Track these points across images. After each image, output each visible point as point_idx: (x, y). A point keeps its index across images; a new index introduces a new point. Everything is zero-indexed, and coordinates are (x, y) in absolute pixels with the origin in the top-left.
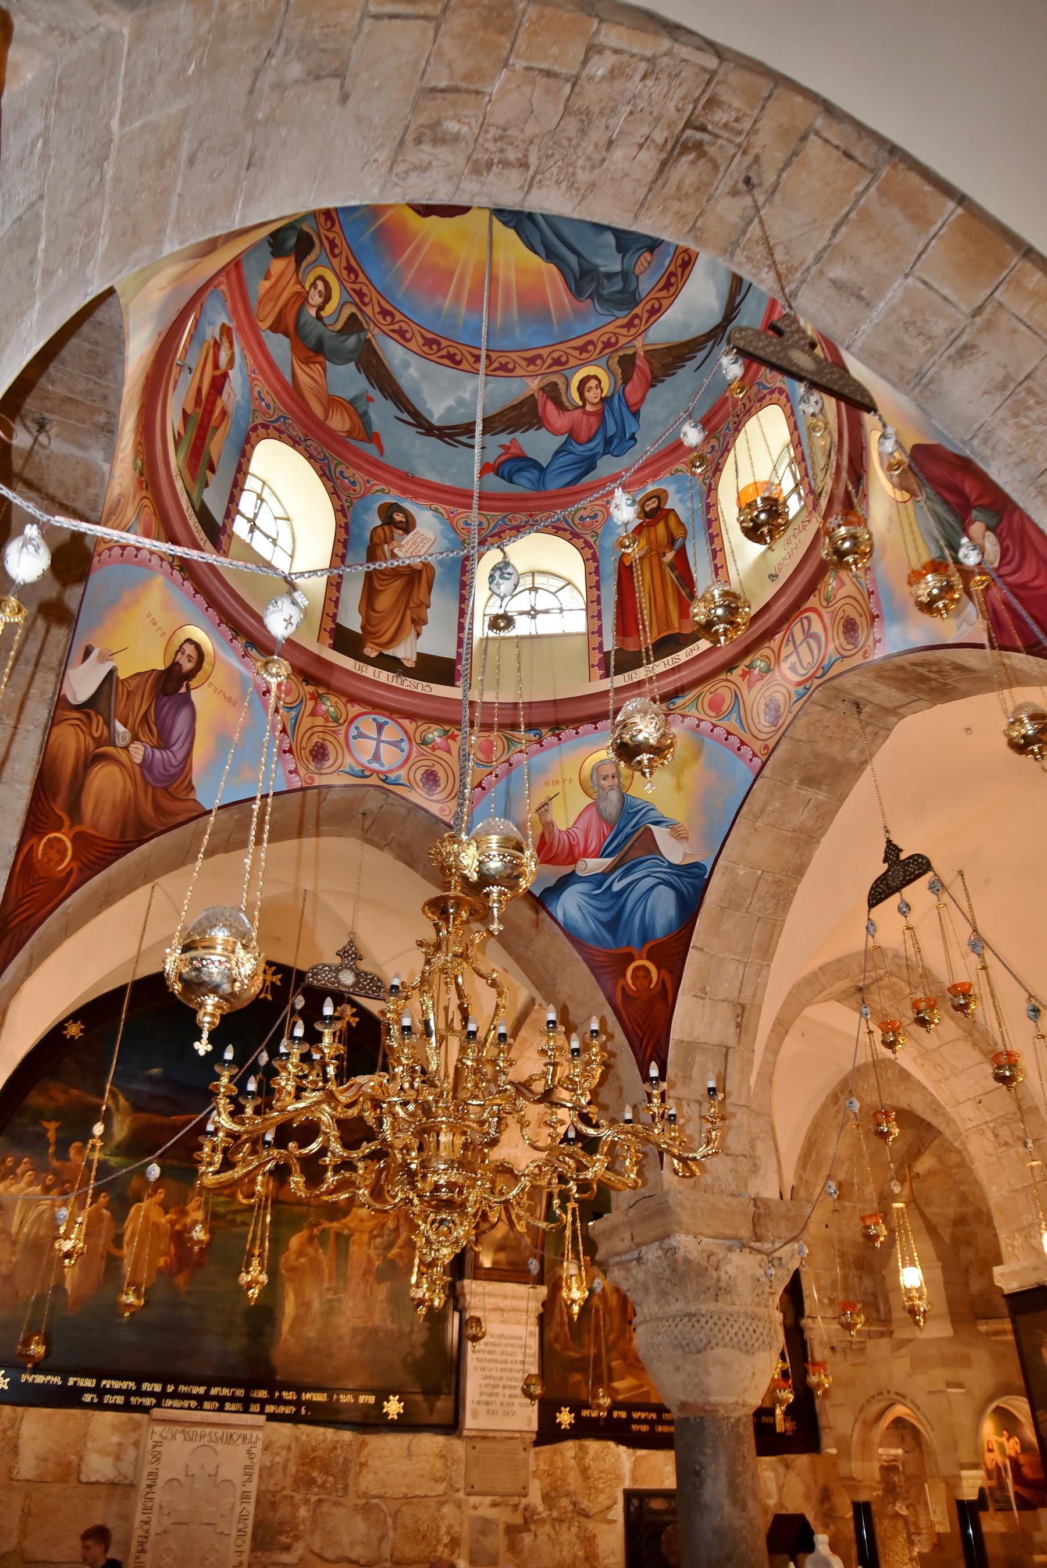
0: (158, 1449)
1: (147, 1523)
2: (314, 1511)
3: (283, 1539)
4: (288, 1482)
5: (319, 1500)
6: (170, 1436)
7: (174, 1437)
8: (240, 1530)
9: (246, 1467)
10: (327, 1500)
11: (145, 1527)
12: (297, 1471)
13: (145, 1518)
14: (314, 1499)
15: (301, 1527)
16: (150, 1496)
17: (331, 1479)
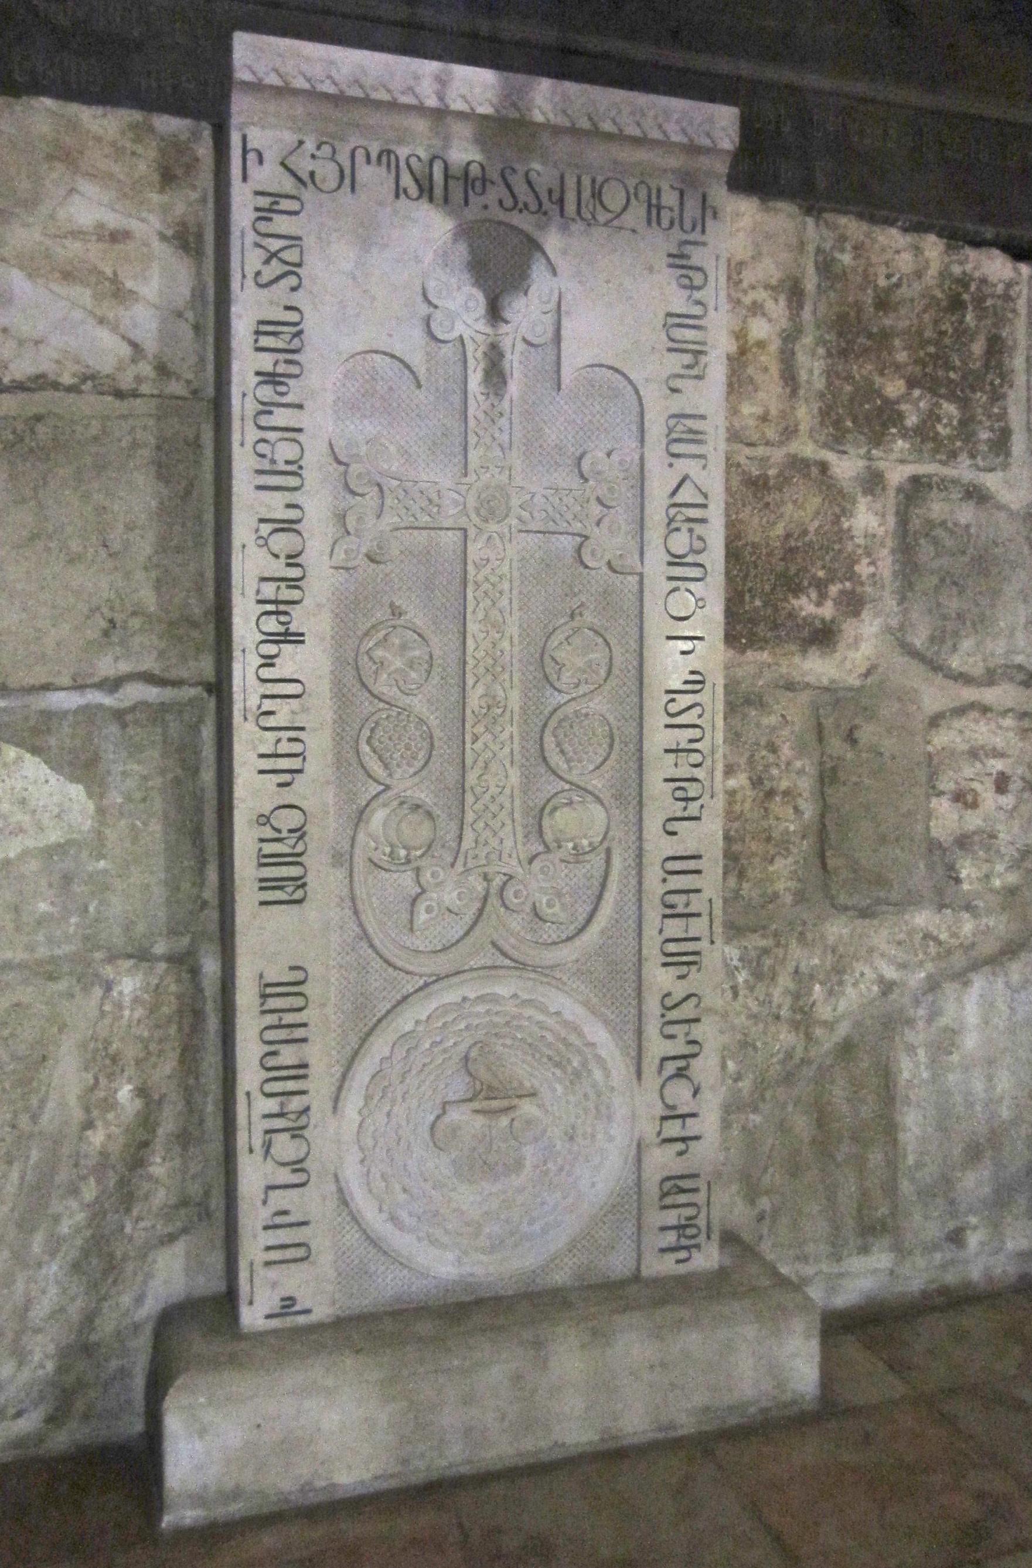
0: (282, 224)
1: (287, 526)
2: (903, 520)
3: (806, 606)
4: (805, 414)
5: (915, 480)
6: (327, 172)
7: (348, 179)
8: (676, 560)
9: (674, 320)
10: (944, 485)
11: (282, 542)
12: (830, 373)
13: (275, 505)
14: (897, 475)
15: (863, 569)
16: (281, 417)
17: (950, 409)
